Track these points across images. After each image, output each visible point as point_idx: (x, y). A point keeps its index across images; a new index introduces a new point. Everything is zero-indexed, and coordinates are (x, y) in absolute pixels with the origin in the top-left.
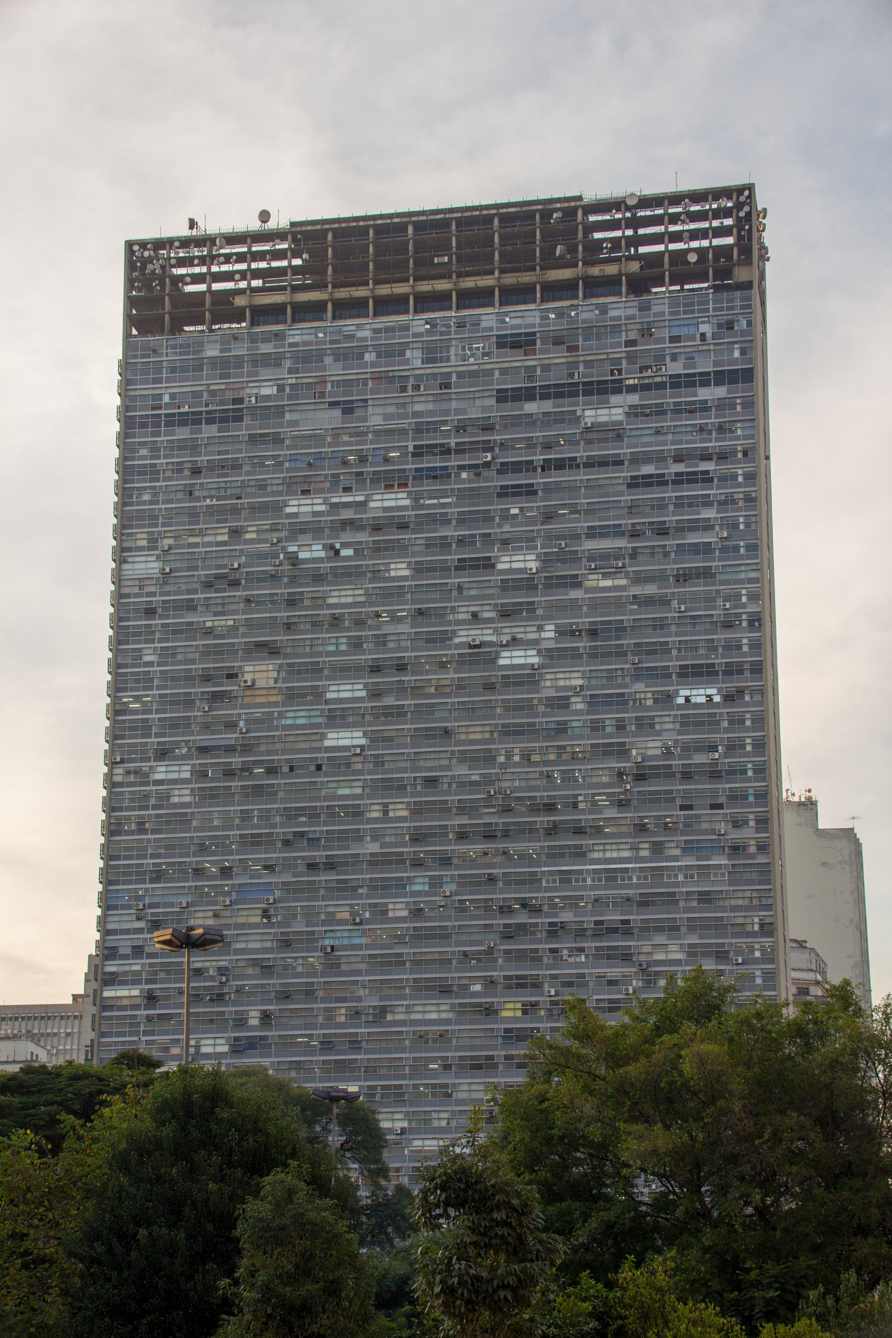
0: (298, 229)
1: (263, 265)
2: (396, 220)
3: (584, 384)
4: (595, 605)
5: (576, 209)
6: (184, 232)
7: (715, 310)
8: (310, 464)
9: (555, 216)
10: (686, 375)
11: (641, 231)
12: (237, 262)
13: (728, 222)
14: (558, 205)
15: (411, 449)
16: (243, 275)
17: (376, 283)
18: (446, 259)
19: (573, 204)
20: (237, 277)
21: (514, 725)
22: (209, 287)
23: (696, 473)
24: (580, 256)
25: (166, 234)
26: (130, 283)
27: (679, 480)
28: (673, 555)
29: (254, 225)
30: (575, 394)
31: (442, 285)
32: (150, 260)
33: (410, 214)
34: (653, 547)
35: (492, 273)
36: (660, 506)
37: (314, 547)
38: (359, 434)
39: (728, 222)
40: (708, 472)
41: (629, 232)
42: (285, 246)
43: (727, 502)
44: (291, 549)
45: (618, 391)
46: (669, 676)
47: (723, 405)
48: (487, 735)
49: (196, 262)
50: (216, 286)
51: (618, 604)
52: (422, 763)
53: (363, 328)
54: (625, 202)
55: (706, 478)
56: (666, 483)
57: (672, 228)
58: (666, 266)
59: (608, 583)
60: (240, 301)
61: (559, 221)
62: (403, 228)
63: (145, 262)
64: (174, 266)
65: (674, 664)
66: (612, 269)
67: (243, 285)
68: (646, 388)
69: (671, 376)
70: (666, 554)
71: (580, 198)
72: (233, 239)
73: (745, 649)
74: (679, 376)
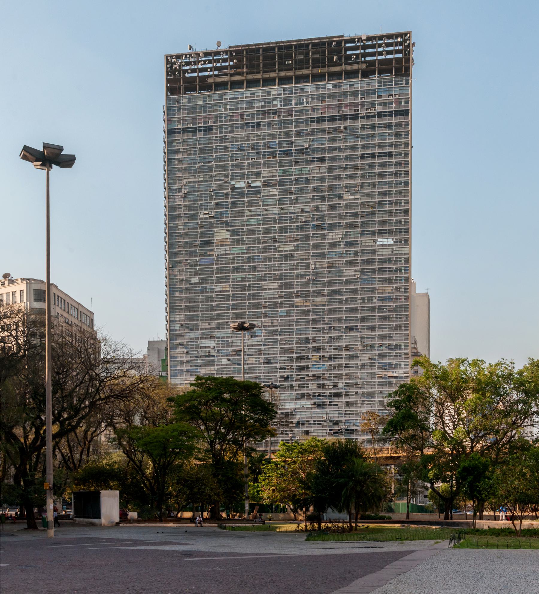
0: (232, 49)
1: (219, 65)
2: (271, 45)
3: (345, 115)
4: (347, 206)
5: (341, 41)
6: (187, 51)
7: (395, 85)
8: (239, 149)
9: (334, 43)
10: (384, 112)
11: (367, 51)
12: (208, 63)
13: (401, 47)
14: (335, 39)
15: (277, 142)
16: (211, 69)
17: (264, 72)
18: (291, 62)
19: (340, 39)
20: (209, 70)
21: (317, 253)
22: (198, 74)
23: (386, 153)
24: (343, 61)
25: (180, 52)
26: (167, 72)
27: (380, 155)
28: (377, 186)
29: (215, 48)
30: (340, 120)
31: (289, 73)
32: (174, 63)
33: (277, 43)
34: (369, 183)
35: (309, 68)
36: (373, 166)
37: (241, 183)
38: (257, 136)
39: (401, 47)
40: (391, 152)
41: (362, 51)
42: (227, 57)
43: (397, 164)
44: (232, 183)
45: (357, 118)
46: (374, 234)
47: (398, 125)
48: (307, 257)
49: (192, 63)
50: (200, 74)
51: (356, 206)
52: (283, 268)
53: (258, 91)
54: (361, 38)
55: (390, 155)
56: (375, 157)
57: (379, 50)
58: (377, 66)
59: (352, 197)
60: (210, 80)
61: (335, 46)
62: (273, 49)
63: (173, 64)
64: (184, 66)
65: (376, 229)
66: (355, 67)
67: (211, 73)
68: (368, 117)
69: (378, 112)
70: (374, 185)
71: (343, 36)
72: (206, 54)
73: (403, 223)
74: (381, 112)
